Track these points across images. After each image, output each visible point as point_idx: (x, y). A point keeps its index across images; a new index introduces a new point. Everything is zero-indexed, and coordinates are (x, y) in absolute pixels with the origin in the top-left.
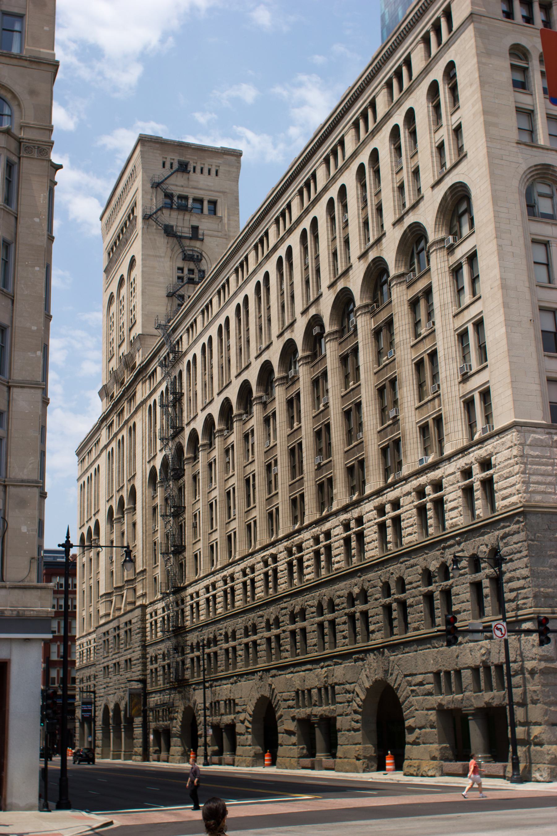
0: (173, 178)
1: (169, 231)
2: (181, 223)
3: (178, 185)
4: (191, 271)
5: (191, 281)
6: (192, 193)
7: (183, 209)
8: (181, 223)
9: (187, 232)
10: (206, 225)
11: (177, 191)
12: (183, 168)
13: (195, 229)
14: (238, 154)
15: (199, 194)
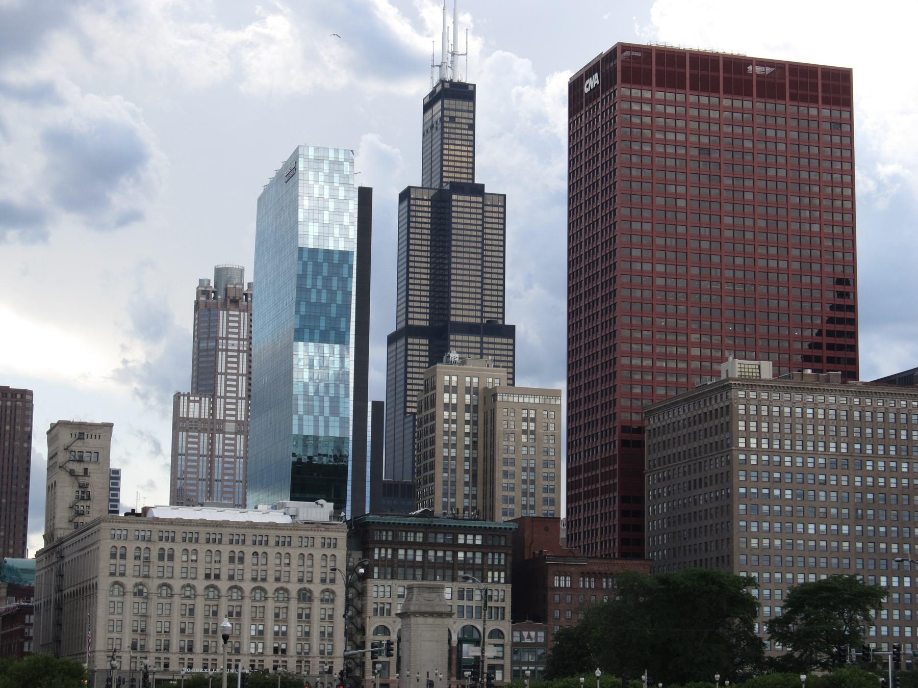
0: (75, 444)
1: (72, 473)
2: (78, 468)
3: (78, 446)
4: (83, 492)
5: (83, 498)
6: (84, 449)
7: (81, 460)
8: (78, 468)
9: (81, 472)
10: (91, 468)
11: (77, 449)
12: (81, 437)
13: (86, 469)
14: (110, 426)
15: (88, 449)
